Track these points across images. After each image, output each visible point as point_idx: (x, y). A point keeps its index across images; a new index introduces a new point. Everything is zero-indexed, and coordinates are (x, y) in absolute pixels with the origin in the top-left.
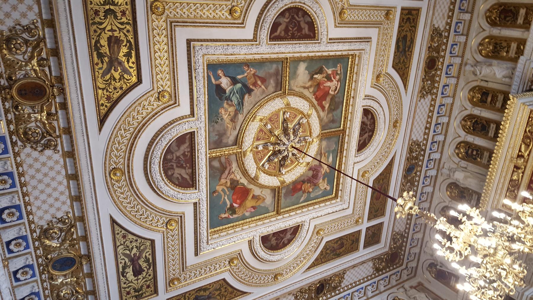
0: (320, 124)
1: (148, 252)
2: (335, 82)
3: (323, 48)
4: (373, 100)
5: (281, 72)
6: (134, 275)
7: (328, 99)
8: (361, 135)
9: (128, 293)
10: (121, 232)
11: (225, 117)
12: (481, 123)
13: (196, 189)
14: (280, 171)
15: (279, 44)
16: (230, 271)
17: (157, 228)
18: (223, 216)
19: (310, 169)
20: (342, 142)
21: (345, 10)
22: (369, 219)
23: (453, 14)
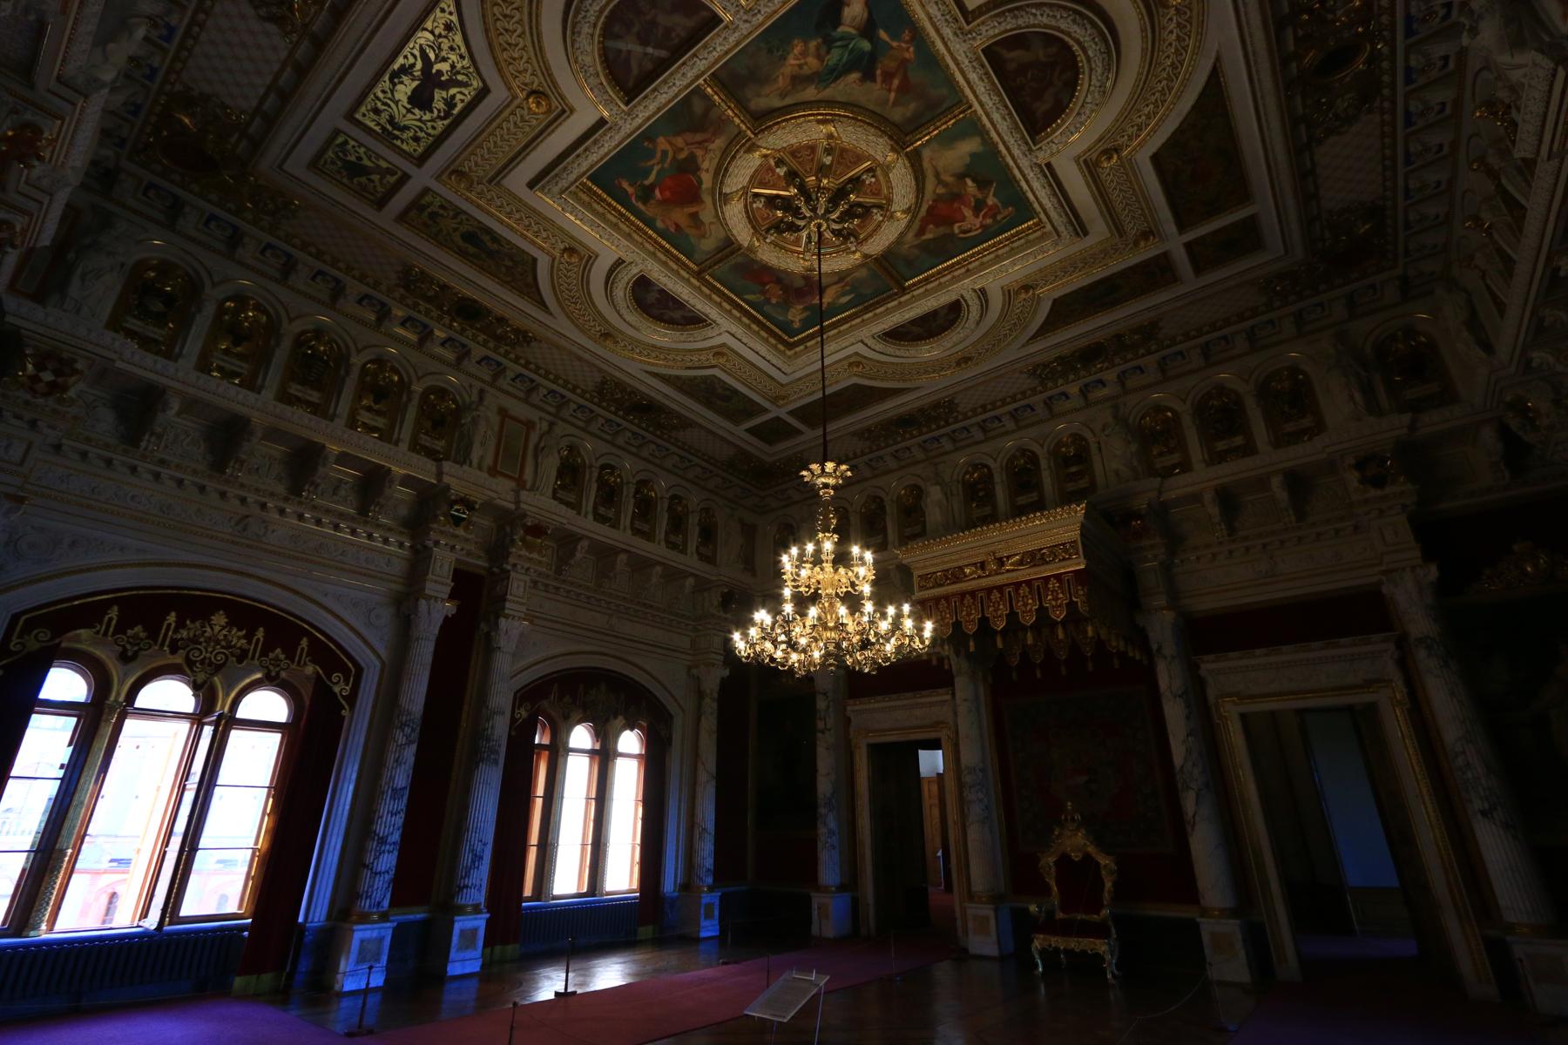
0: (890, 245)
1: (464, 95)
2: (977, 222)
3: (1024, 163)
4: (982, 306)
5: (939, 111)
6: (409, 98)
7: (942, 230)
8: (913, 322)
9: (377, 111)
10: (451, 14)
11: (792, 61)
13: (627, 104)
14: (767, 231)
15: (987, 73)
16: (554, 259)
17: (511, 79)
18: (625, 185)
19: (806, 278)
20: (884, 300)
21: (1115, 157)
22: (791, 413)
23: (1195, 337)
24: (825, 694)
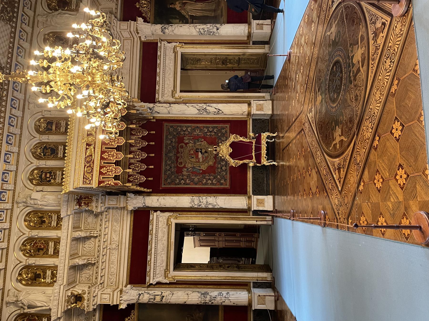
12: (49, 148)
24: (140, 295)
